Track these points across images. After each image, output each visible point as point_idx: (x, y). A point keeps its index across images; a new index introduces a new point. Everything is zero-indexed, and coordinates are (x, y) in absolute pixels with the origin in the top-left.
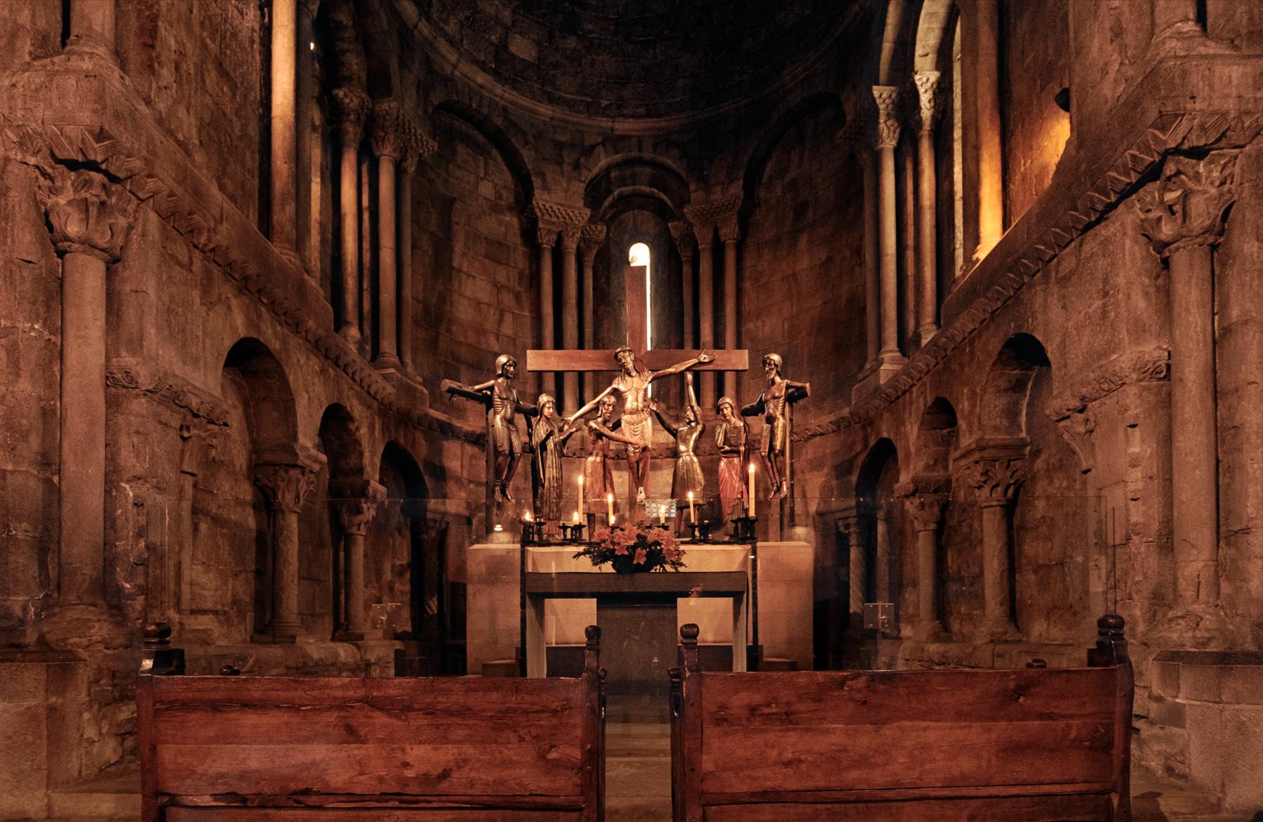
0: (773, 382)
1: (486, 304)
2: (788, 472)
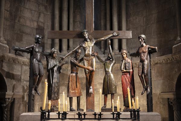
0: (142, 46)
1: (34, 10)
2: (150, 84)
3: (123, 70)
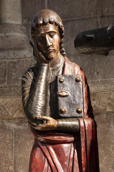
3: (42, 121)
